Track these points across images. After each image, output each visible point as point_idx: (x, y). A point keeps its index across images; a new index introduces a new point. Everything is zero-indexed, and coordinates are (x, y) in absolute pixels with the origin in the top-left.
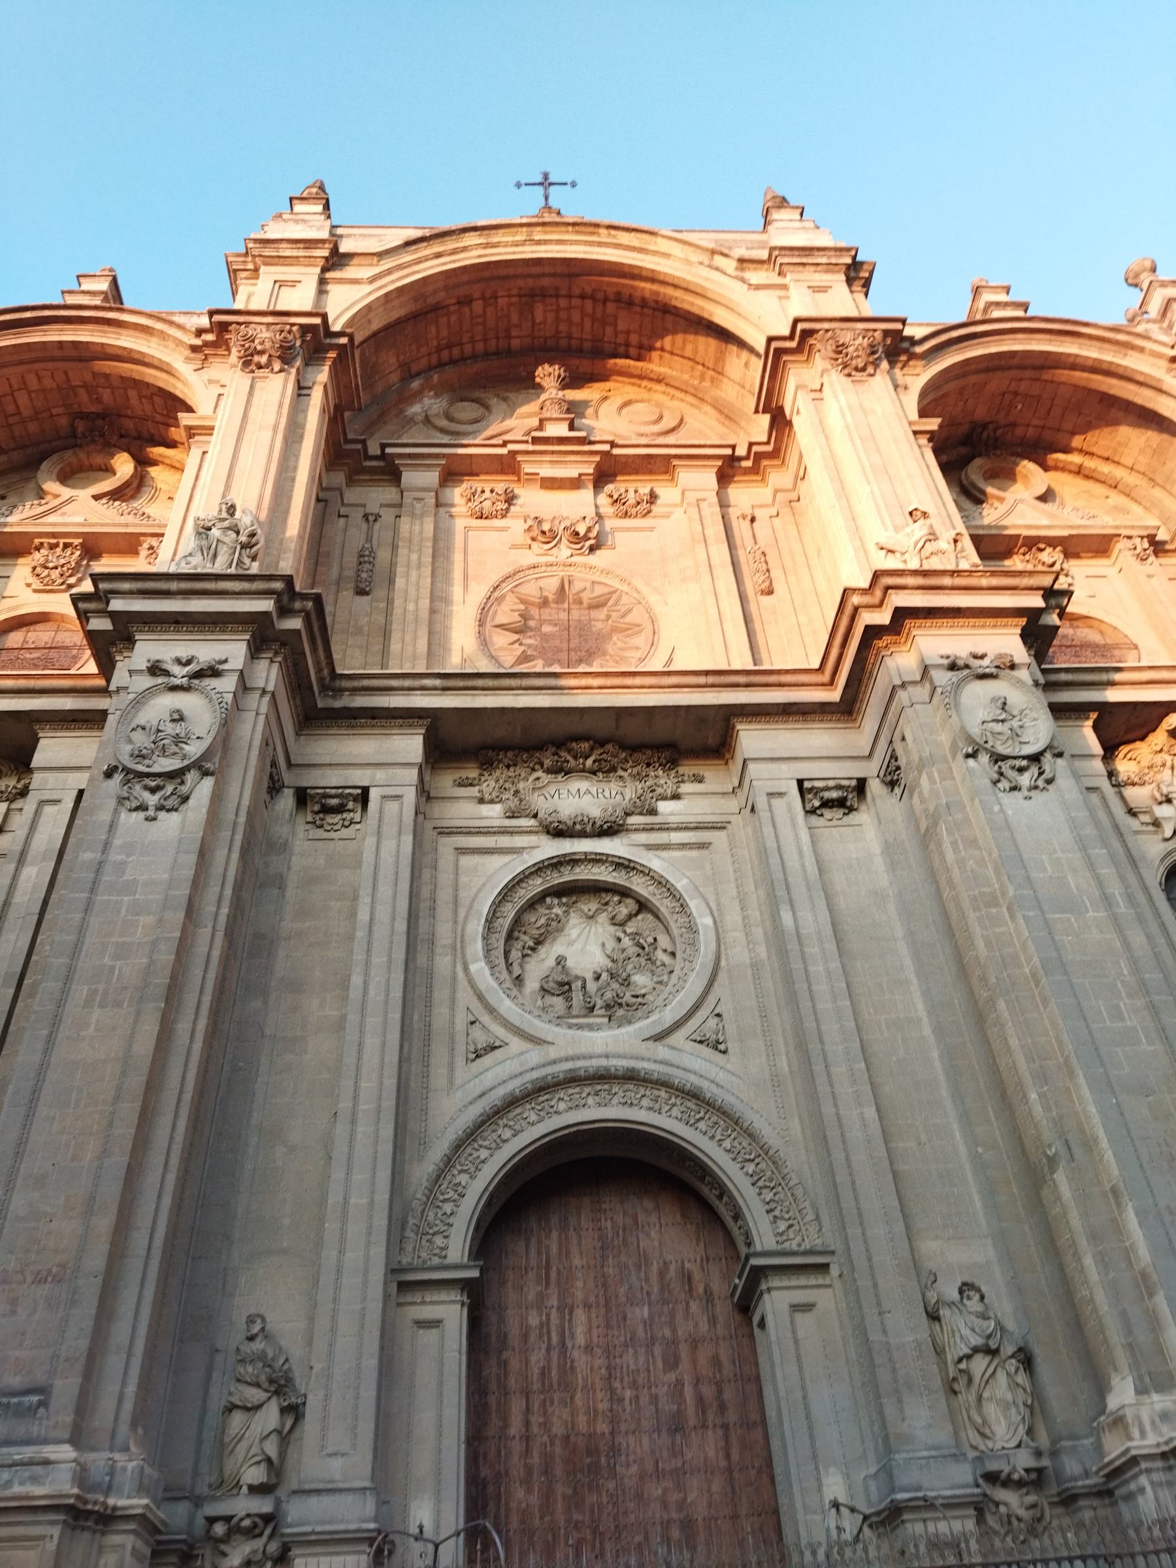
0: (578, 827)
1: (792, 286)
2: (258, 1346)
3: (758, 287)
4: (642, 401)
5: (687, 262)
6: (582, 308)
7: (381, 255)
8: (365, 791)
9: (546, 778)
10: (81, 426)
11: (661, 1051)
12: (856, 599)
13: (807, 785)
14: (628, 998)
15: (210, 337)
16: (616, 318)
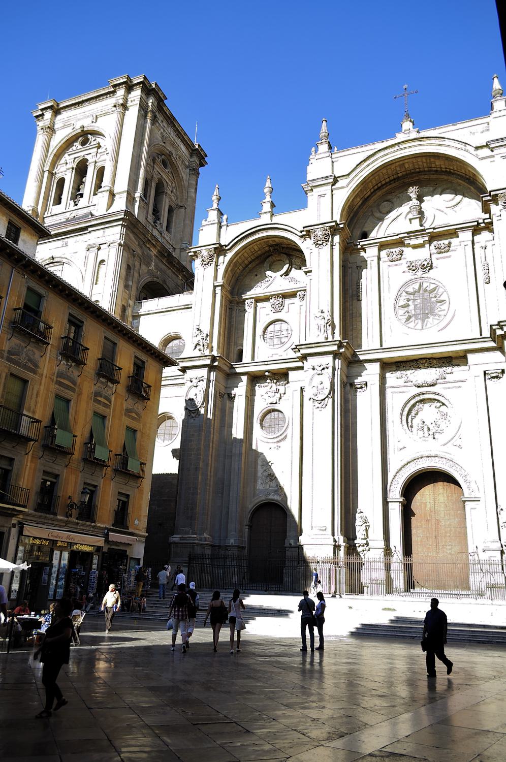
0: (424, 385)
1: (495, 156)
2: (361, 514)
3: (482, 159)
4: (447, 189)
5: (458, 149)
6: (423, 162)
7: (349, 174)
8: (366, 383)
9: (413, 371)
10: (271, 249)
11: (445, 448)
12: (494, 327)
13: (487, 372)
14: (439, 431)
15: (304, 233)
16: (435, 162)
